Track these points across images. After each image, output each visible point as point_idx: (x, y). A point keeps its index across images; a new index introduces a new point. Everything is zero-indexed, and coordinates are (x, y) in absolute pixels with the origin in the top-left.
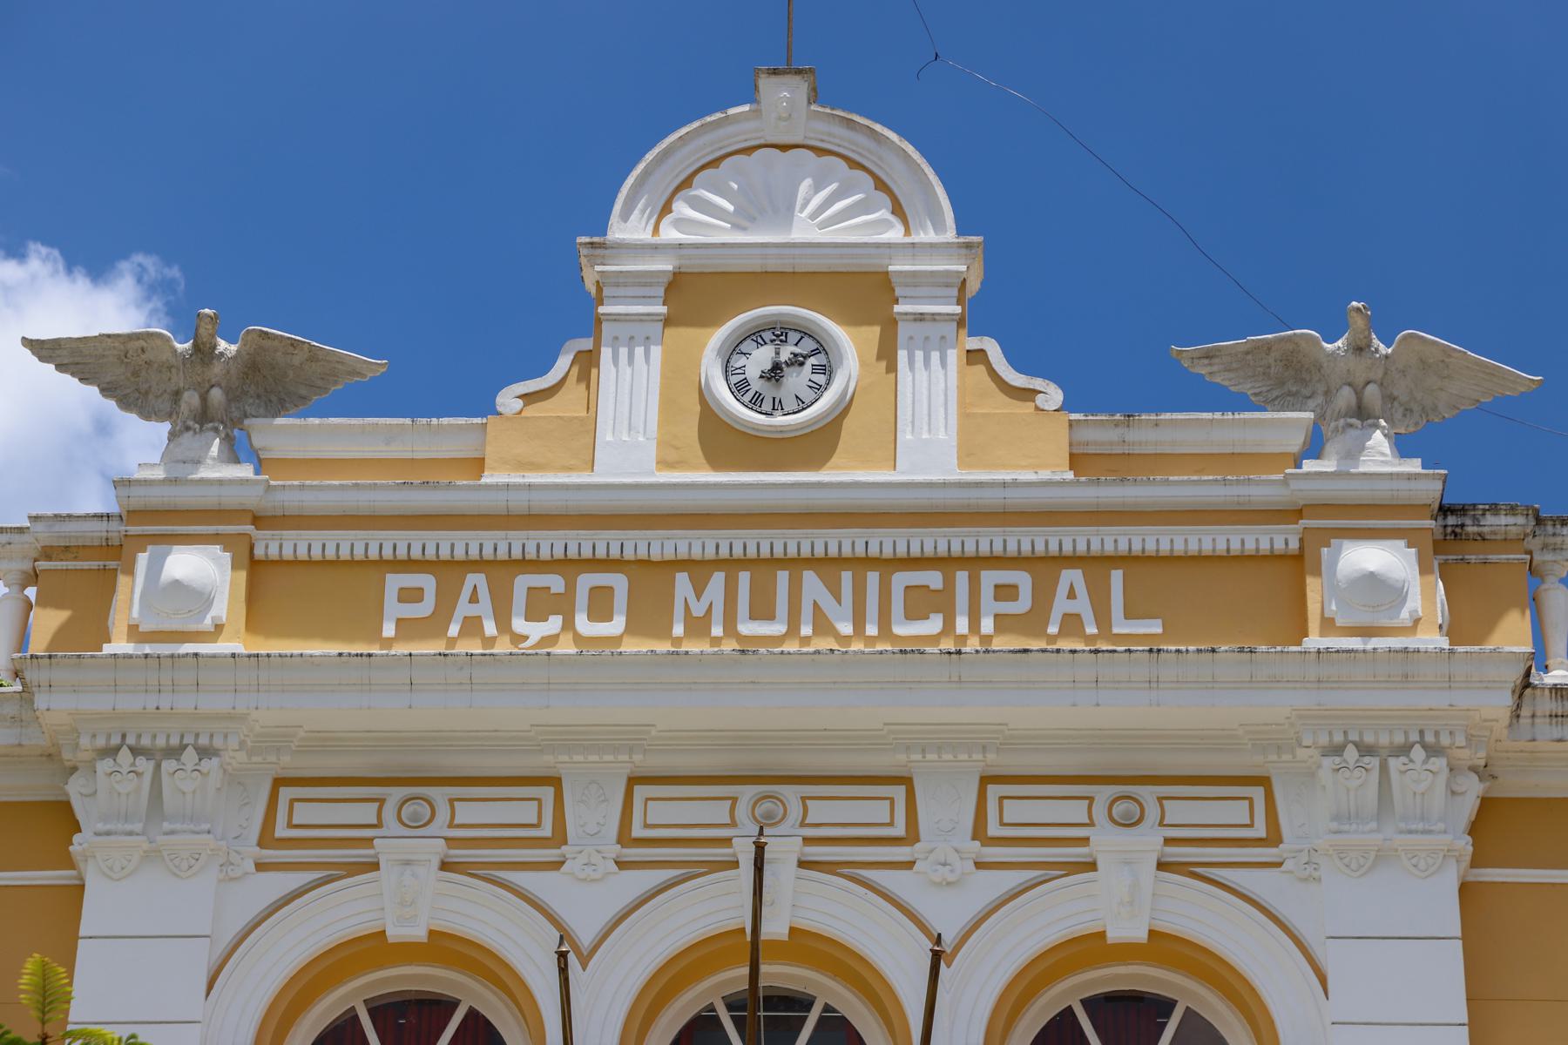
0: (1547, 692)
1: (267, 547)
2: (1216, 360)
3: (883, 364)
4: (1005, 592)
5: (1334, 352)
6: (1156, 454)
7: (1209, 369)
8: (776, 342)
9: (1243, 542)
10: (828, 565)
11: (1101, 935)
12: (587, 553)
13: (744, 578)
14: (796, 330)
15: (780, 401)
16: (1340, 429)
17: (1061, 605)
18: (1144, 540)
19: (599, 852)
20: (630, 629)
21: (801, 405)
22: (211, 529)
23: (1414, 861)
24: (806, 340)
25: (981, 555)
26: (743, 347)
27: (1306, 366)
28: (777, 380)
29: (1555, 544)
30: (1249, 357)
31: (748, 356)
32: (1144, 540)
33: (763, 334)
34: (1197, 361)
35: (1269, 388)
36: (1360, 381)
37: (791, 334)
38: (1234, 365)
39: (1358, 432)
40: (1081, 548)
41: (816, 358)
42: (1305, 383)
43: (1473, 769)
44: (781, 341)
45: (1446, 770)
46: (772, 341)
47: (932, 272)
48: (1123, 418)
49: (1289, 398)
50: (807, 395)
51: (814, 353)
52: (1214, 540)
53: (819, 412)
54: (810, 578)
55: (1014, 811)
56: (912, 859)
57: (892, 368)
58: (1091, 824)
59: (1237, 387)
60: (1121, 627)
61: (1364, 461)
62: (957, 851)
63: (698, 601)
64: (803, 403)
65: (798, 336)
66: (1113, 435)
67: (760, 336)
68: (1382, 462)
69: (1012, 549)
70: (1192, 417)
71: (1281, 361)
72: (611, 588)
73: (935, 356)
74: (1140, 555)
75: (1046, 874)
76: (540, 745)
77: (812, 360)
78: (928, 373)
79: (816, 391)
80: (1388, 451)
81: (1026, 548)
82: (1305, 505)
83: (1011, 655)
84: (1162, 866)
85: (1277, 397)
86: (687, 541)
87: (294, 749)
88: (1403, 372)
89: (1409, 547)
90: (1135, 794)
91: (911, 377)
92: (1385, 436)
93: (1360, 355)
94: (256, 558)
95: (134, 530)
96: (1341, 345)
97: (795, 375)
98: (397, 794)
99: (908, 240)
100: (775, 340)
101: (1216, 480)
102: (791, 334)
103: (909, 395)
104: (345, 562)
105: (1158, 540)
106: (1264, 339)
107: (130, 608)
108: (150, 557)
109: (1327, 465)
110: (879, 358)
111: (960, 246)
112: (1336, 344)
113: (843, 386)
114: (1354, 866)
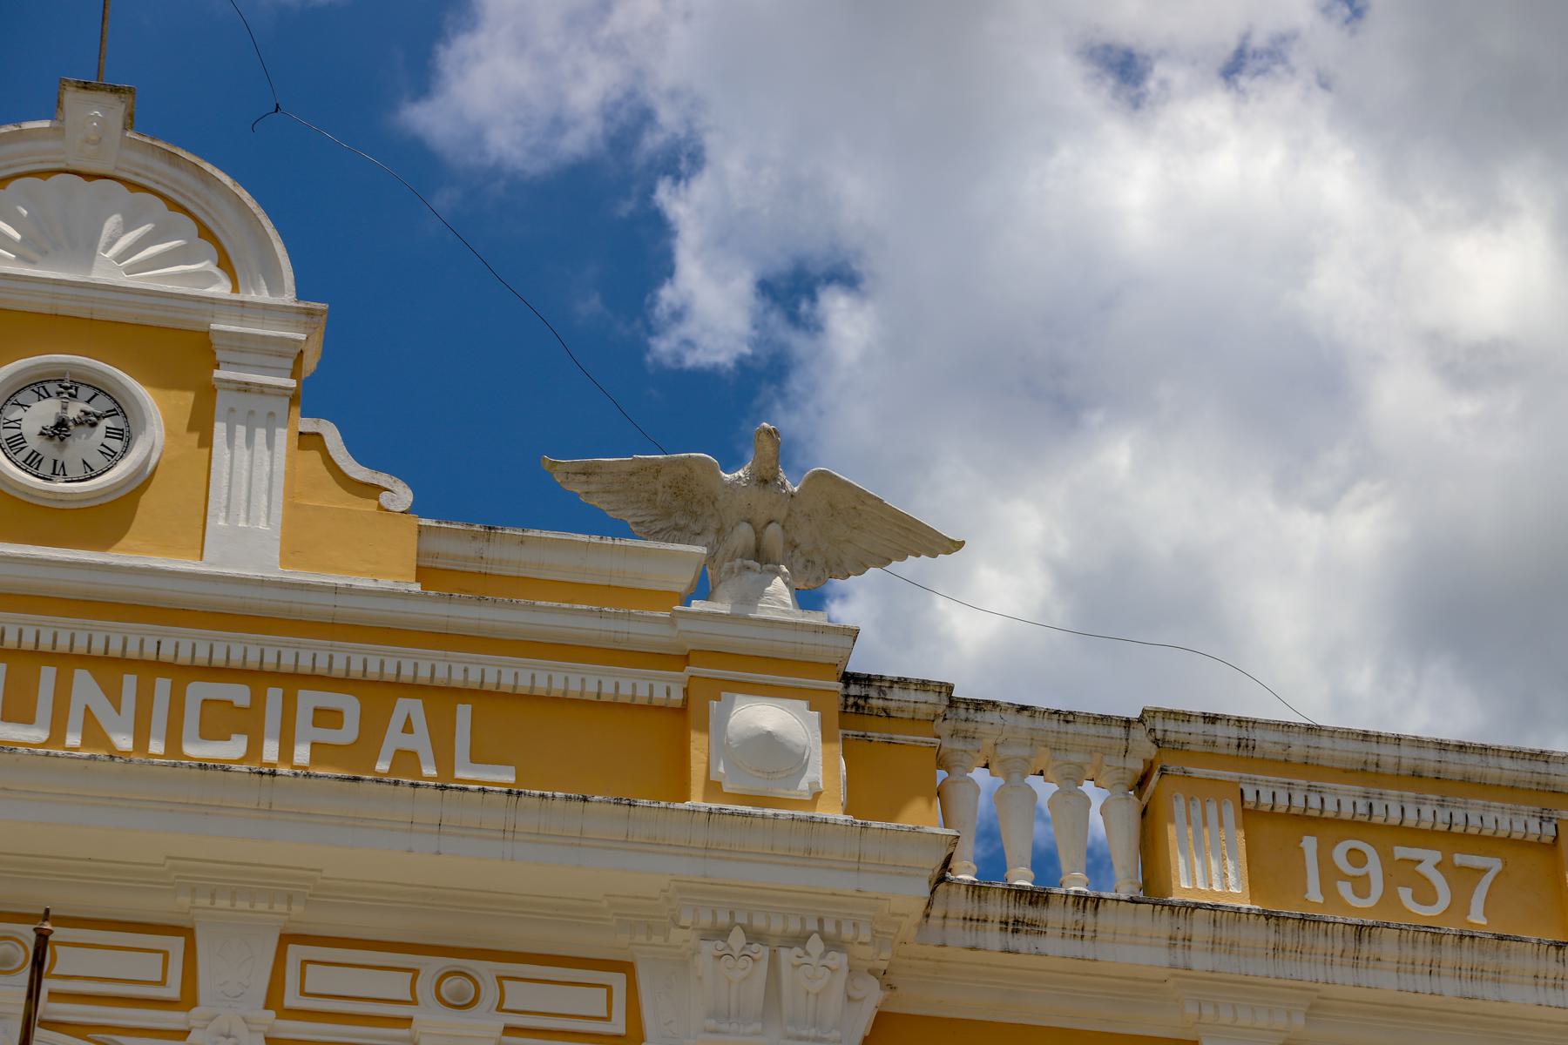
0: (963, 888)
2: (592, 479)
3: (195, 436)
4: (327, 717)
5: (733, 483)
6: (518, 577)
7: (585, 488)
8: (64, 395)
9: (617, 686)
10: (107, 666)
14: (89, 386)
15: (63, 465)
16: (736, 570)
17: (394, 739)
18: (499, 672)
21: (90, 473)
24: (101, 397)
25: (300, 671)
26: (20, 398)
27: (699, 497)
28: (62, 439)
30: (634, 479)
31: (26, 408)
32: (499, 672)
33: (48, 386)
34: (573, 476)
35: (653, 518)
37: (82, 389)
38: (616, 487)
39: (757, 576)
40: (424, 674)
41: (111, 420)
42: (694, 516)
43: (872, 972)
44: (70, 395)
45: (846, 969)
46: (59, 394)
47: (264, 337)
48: (482, 530)
49: (675, 533)
50: (98, 461)
51: (110, 414)
52: (583, 680)
53: (111, 483)
56: (187, 1028)
57: (206, 442)
58: (414, 1002)
59: (616, 513)
61: (762, 608)
62: (245, 1020)
64: (92, 470)
65: (91, 392)
66: (468, 549)
67: (43, 387)
68: (783, 611)
69: (339, 667)
70: (564, 537)
71: (670, 487)
73: (261, 434)
74: (494, 689)
77: (107, 422)
78: (249, 452)
79: (109, 458)
80: (789, 600)
81: (356, 668)
85: (662, 530)
90: (470, 969)
91: (229, 455)
92: (786, 584)
93: (764, 487)
96: (741, 475)
97: (84, 436)
99: (235, 297)
100: (62, 393)
101: (591, 611)
102: (82, 389)
103: (225, 476)
105: (516, 674)
106: (653, 459)
109: (722, 607)
110: (191, 428)
111: (299, 311)
112: (736, 474)
113: (145, 455)
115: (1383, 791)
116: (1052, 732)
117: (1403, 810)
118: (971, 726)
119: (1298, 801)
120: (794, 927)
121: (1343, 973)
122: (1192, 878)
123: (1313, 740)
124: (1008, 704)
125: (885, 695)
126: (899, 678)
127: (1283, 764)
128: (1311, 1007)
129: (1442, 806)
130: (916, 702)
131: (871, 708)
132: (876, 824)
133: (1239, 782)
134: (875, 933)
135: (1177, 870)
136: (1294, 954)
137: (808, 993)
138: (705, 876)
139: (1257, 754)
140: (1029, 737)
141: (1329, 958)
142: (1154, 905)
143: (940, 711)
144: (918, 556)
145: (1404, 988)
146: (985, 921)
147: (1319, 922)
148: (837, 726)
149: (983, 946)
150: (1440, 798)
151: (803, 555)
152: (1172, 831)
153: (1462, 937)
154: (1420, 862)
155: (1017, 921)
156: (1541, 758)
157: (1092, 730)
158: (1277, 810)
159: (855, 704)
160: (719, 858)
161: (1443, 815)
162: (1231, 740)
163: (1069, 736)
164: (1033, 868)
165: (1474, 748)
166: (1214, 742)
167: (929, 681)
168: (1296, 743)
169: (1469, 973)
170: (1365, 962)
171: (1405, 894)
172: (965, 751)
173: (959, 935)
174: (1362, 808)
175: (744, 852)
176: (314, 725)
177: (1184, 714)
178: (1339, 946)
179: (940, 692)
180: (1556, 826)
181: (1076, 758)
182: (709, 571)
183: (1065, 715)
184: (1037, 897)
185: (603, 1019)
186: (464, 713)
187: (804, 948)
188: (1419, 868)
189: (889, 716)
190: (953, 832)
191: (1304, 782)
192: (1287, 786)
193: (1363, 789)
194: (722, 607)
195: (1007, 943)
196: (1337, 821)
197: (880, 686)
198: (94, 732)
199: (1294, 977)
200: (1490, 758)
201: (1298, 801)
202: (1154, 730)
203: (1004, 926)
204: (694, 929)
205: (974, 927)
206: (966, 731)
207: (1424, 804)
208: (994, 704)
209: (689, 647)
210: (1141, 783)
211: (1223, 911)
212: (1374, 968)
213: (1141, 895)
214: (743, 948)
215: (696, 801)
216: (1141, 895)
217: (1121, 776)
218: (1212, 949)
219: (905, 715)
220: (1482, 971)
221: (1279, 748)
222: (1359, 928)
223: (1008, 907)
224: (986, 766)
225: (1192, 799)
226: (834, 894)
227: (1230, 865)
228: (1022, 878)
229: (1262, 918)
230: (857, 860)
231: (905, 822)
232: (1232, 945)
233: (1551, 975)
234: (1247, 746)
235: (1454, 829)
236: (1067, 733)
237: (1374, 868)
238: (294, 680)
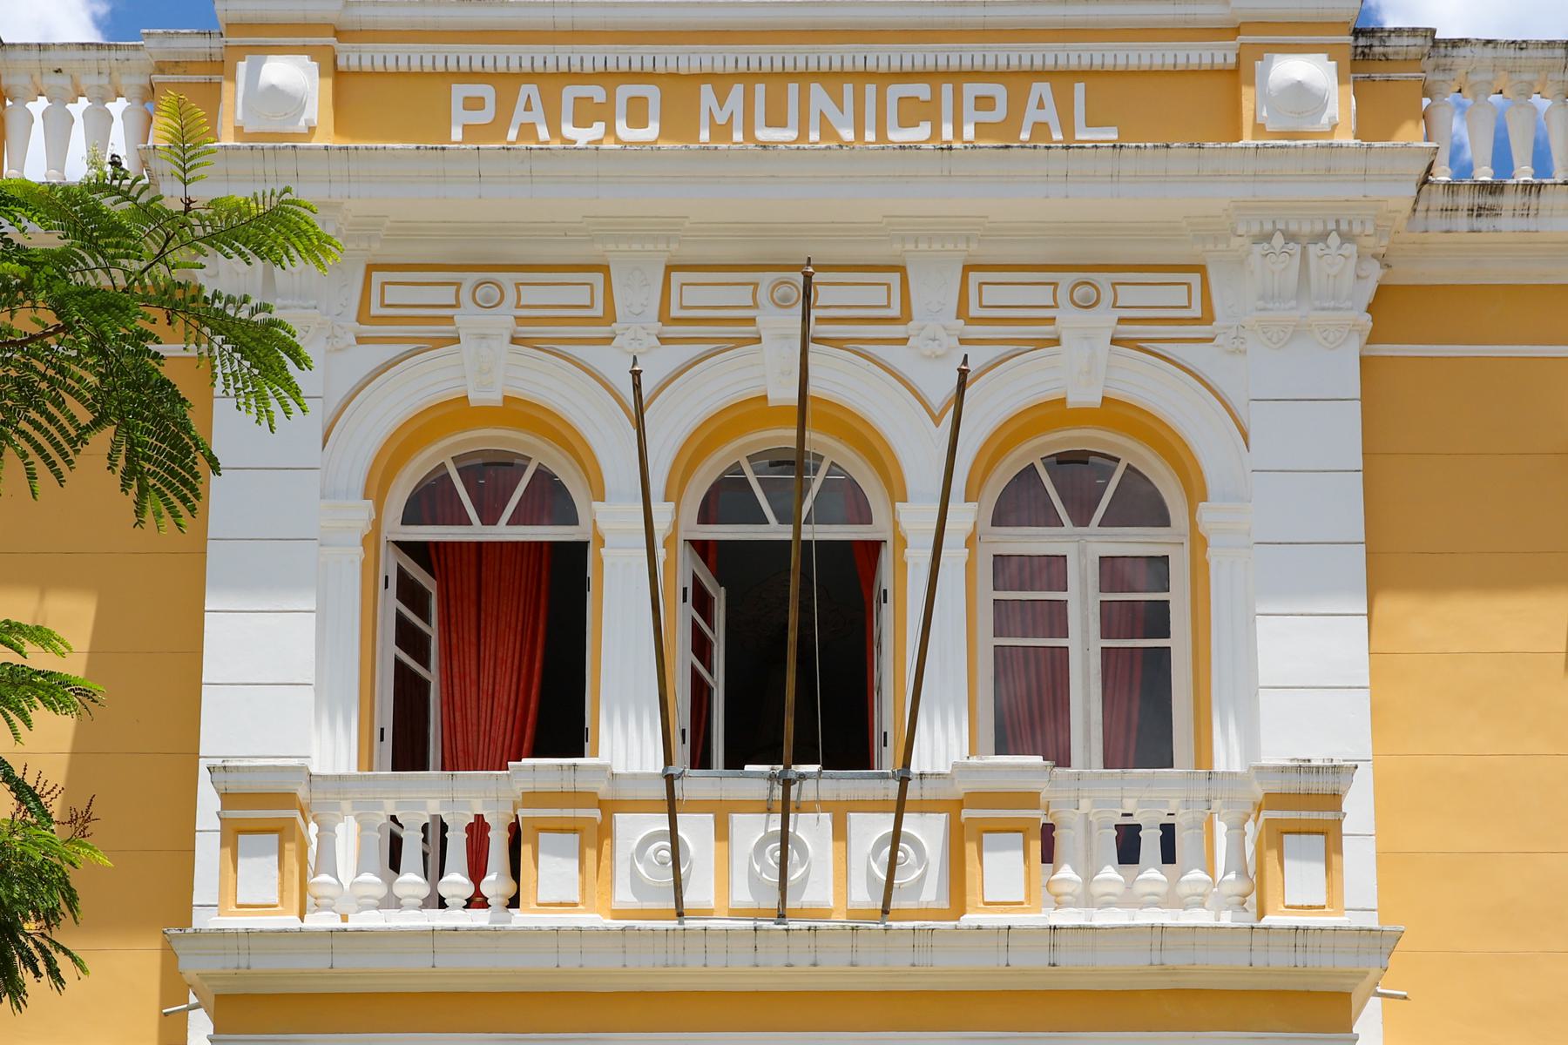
0: (1441, 187)
1: (348, 59)
4: (984, 103)
11: (1063, 401)
12: (624, 67)
13: (760, 89)
17: (1032, 115)
19: (643, 328)
20: (663, 134)
22: (299, 41)
23: (1325, 334)
25: (963, 69)
29: (1445, 65)
40: (1050, 62)
43: (1374, 256)
45: (1356, 255)
54: (816, 89)
55: (992, 295)
58: (1056, 306)
60: (1083, 135)
62: (945, 329)
63: (721, 110)
72: (646, 98)
74: (1100, 69)
75: (1018, 349)
76: (590, 236)
83: (994, 150)
84: (1114, 341)
86: (710, 56)
87: (383, 237)
89: (1329, 60)
94: (339, 69)
95: (234, 41)
98: (472, 278)
104: (416, 73)
105: (1115, 56)
107: (235, 112)
108: (248, 64)
114: (1274, 340)
116: (1510, 58)
118: (1449, 61)
120: (1319, 227)
124: (1477, 39)
125: (1385, 42)
130: (1407, 46)
131: (1374, 55)
132: (1377, 144)
134: (1377, 226)
137: (1328, 276)
138: (1254, 196)
146: (1457, 210)
148: (1349, 71)
149: (1454, 229)
155: (1480, 208)
157: (1540, 53)
159: (1363, 52)
172: (1443, 81)
173: (1437, 222)
175: (1281, 175)
176: (976, 109)
179: (1426, 36)
181: (1526, 77)
183: (1520, 44)
184: (1494, 189)
185: (1185, 307)
186: (1079, 89)
187: (1326, 243)
189: (1387, 60)
195: (1473, 225)
197: (1381, 36)
198: (827, 130)
203: (1471, 212)
205: (1448, 217)
208: (1466, 41)
214: (1283, 247)
219: (1400, 57)
223: (1474, 197)
226: (1347, 201)
228: (1485, 175)
230: (1363, 173)
231: (1399, 141)
236: (1521, 58)
238: (959, 76)
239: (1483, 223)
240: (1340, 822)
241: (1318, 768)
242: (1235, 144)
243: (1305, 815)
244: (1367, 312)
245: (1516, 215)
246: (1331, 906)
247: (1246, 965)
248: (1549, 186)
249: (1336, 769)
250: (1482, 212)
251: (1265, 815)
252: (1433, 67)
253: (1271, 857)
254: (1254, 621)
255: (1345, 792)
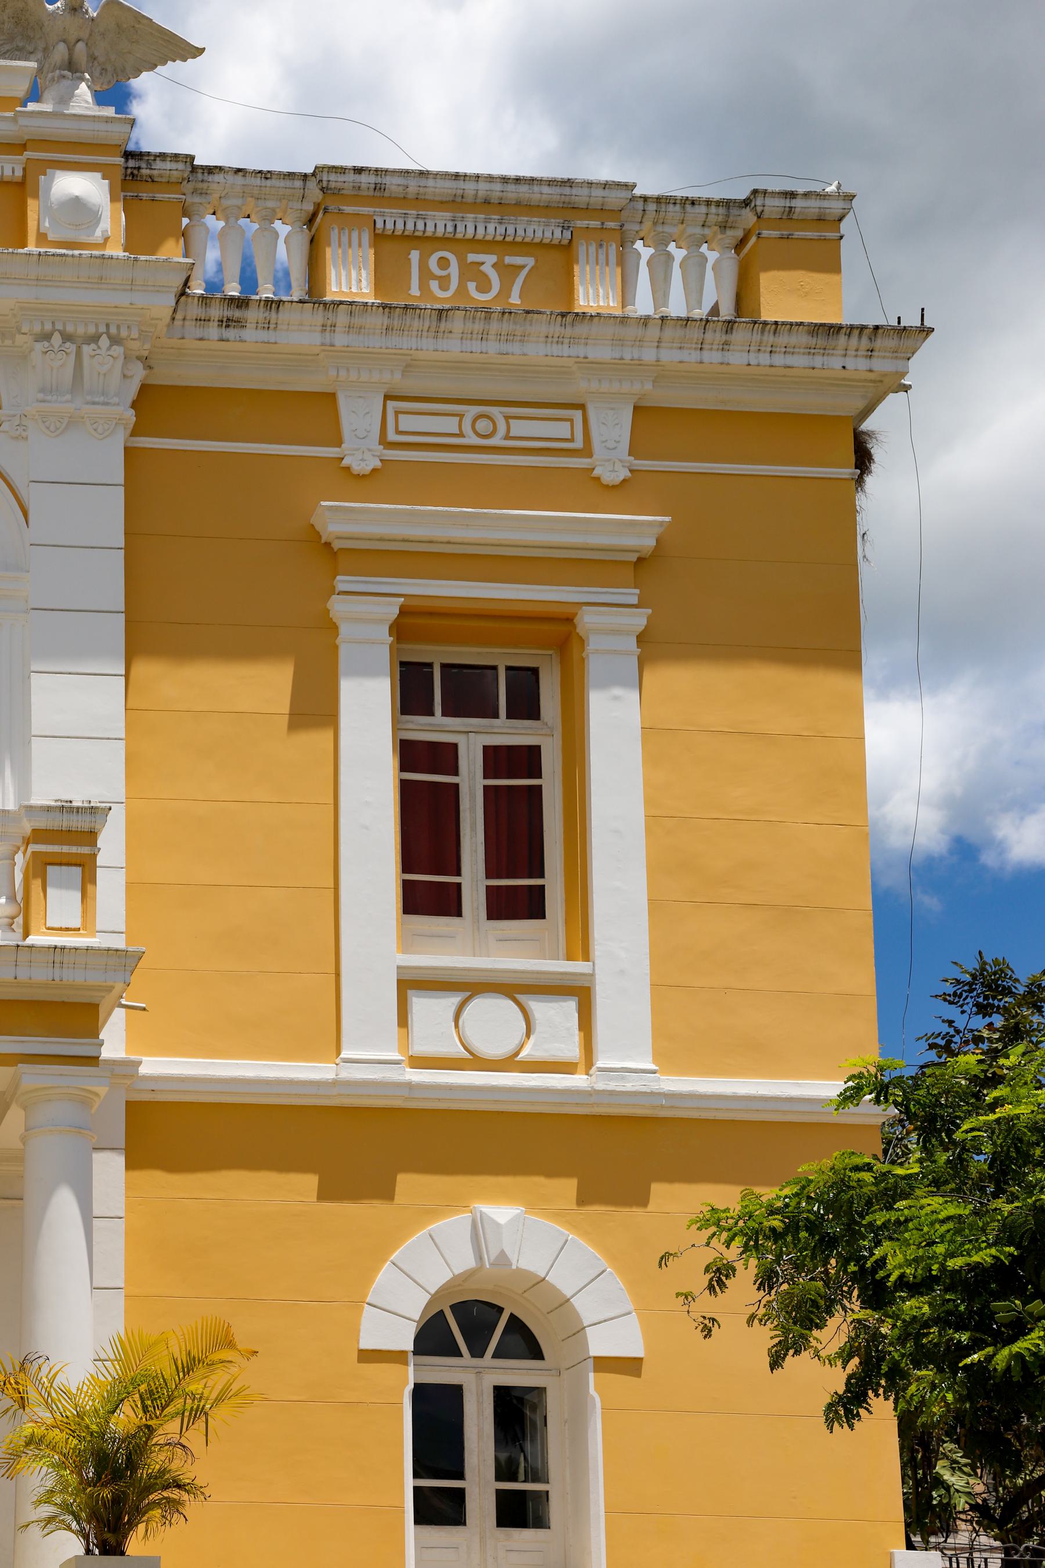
0: (196, 299)
16: (56, 79)
23: (95, 426)
36: (72, 39)
39: (69, 82)
42: (29, 39)
43: (138, 358)
45: (123, 357)
49: (17, 53)
61: (73, 106)
68: (86, 108)
80: (90, 99)
82: (29, 140)
85: (8, 51)
88: (103, 35)
92: (89, 87)
114: (52, 428)
115: (464, 215)
116: (257, 186)
117: (476, 227)
118: (205, 185)
119: (410, 226)
120: (91, 330)
121: (428, 343)
122: (339, 284)
123: (423, 182)
124: (230, 167)
125: (151, 166)
126: (160, 153)
127: (402, 201)
128: (406, 367)
129: (501, 223)
130: (170, 170)
131: (142, 176)
132: (143, 258)
133: (374, 215)
134: (141, 331)
135: (330, 279)
136: (398, 332)
137: (99, 374)
138: (37, 299)
139: (387, 194)
140: (242, 191)
141: (420, 333)
142: (314, 303)
143: (186, 175)
144: (174, 61)
145: (464, 350)
146: (209, 320)
147: (416, 309)
149: (206, 337)
150: (499, 217)
151: (100, 65)
152: (329, 252)
153: (504, 313)
154: (483, 263)
156: (568, 184)
157: (282, 183)
158: (396, 233)
159: (132, 173)
160: (46, 286)
161: (501, 230)
162: (371, 185)
163: (267, 188)
164: (241, 284)
165: (526, 180)
166: (359, 187)
167: (179, 154)
168: (412, 184)
169: (506, 337)
170: (442, 334)
171: (472, 286)
172: (201, 203)
173: (192, 330)
174: (450, 229)
175: (60, 281)
177: (342, 168)
178: (427, 324)
179: (186, 162)
180: (572, 232)
181: (270, 204)
182: (39, 80)
184: (241, 303)
187: (97, 344)
188: (482, 268)
189: (153, 181)
190: (190, 261)
191: (414, 212)
192: (403, 215)
193: (452, 214)
194: (46, 107)
195: (222, 334)
196: (434, 239)
199: (397, 347)
200: (535, 186)
201: (410, 226)
202: (322, 181)
204: (30, 335)
205: (202, 326)
206: (202, 189)
207: (490, 222)
208: (220, 169)
209: (26, 137)
210: (311, 221)
211: (357, 306)
212: (447, 338)
213: (307, 298)
214: (60, 346)
215: (32, 248)
216: (307, 298)
217: (299, 215)
218: (348, 332)
219: (164, 180)
220: (514, 335)
221: (401, 188)
222: (440, 311)
224: (214, 214)
225: (343, 229)
226: (116, 307)
227: (364, 273)
228: (233, 290)
229: (381, 308)
230: (130, 283)
231: (161, 256)
232: (360, 328)
233: (556, 335)
234: (380, 189)
235: (508, 239)
236: (266, 187)
237: (454, 270)
239: (231, 333)
240: (95, 856)
241: (78, 808)
242: (20, 251)
243: (65, 849)
244: (131, 408)
245: (259, 327)
246: (85, 929)
247: (11, 978)
248: (286, 303)
249: (93, 810)
250: (230, 324)
251: (33, 848)
252: (192, 191)
253: (36, 884)
254: (29, 677)
255: (100, 830)
